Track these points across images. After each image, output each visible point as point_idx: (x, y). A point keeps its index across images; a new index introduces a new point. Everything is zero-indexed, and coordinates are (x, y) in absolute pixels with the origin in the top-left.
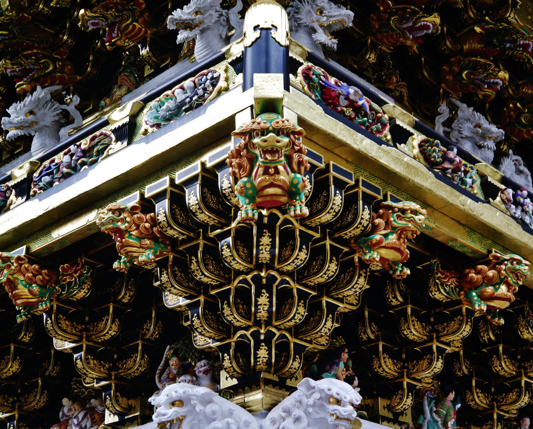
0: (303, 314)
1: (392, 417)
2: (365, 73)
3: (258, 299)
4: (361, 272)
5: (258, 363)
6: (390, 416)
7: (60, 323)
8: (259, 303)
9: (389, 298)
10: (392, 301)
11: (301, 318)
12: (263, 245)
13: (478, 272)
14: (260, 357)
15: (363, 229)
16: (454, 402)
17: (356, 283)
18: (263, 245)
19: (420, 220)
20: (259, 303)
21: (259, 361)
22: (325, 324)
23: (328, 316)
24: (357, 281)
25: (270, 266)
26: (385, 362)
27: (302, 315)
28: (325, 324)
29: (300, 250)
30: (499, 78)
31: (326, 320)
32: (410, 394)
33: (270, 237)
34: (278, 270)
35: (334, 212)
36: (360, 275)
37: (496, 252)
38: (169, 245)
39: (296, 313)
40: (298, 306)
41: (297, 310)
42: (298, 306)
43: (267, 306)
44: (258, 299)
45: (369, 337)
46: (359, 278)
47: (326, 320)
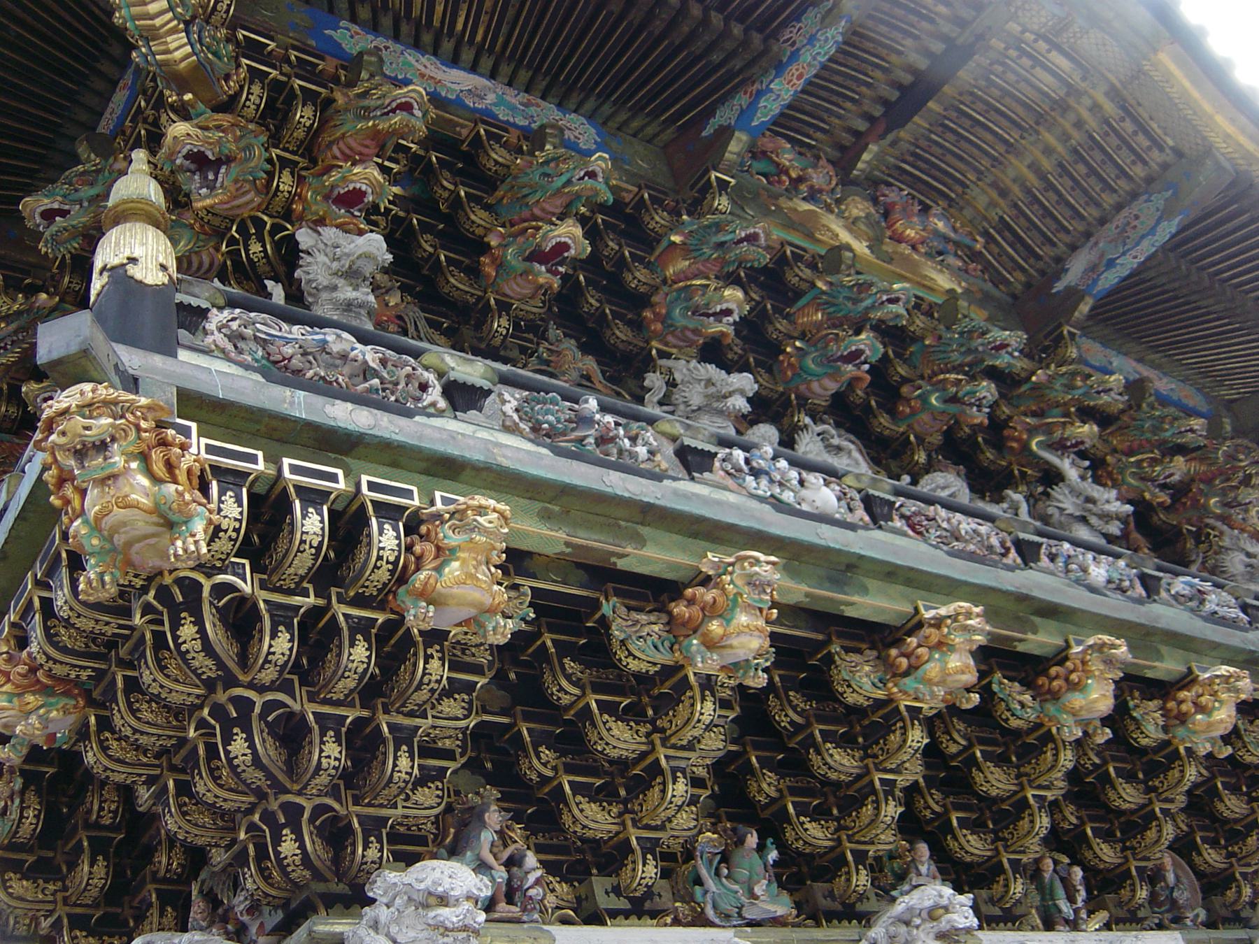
0: (338, 756)
1: (629, 906)
2: (502, 353)
3: (229, 748)
4: (429, 651)
5: (290, 869)
6: (623, 904)
7: (11, 887)
8: (232, 755)
9: (552, 694)
10: (559, 699)
11: (337, 763)
12: (185, 642)
13: (691, 602)
14: (286, 858)
15: (390, 567)
16: (761, 848)
17: (424, 674)
18: (185, 642)
19: (490, 522)
20: (232, 755)
21: (288, 865)
22: (395, 765)
23: (397, 749)
24: (425, 668)
25: (230, 681)
26: (582, 811)
27: (336, 759)
28: (395, 765)
29: (273, 636)
30: (727, 301)
31: (396, 758)
32: (649, 856)
33: (194, 623)
34: (251, 686)
35: (311, 547)
36: (428, 658)
37: (712, 559)
38: (79, 695)
39: (320, 757)
40: (322, 742)
41: (321, 751)
42: (322, 742)
43: (249, 758)
44: (229, 748)
45: (540, 775)
46: (426, 662)
47: (396, 758)
